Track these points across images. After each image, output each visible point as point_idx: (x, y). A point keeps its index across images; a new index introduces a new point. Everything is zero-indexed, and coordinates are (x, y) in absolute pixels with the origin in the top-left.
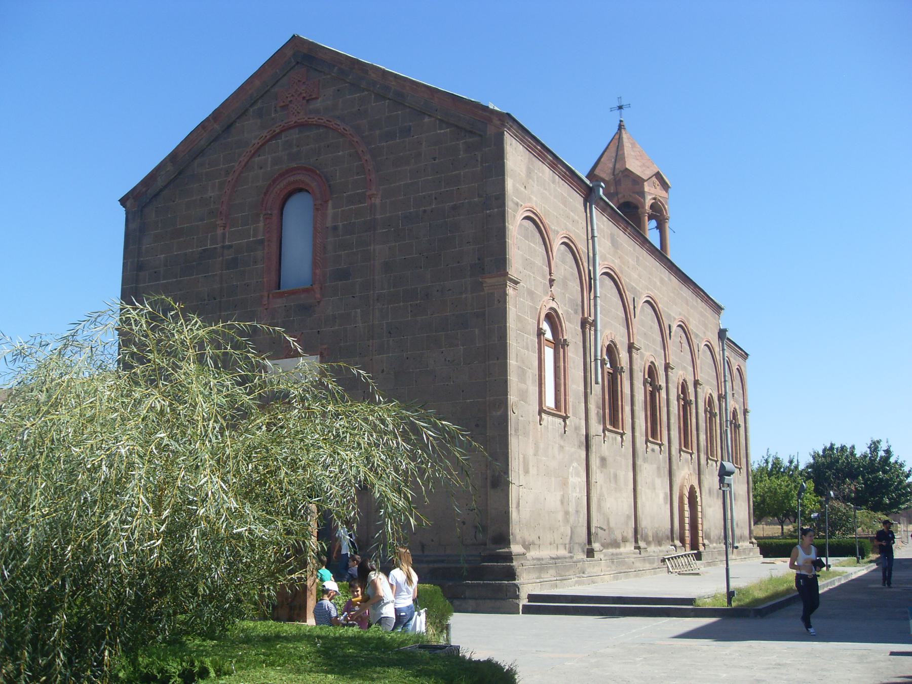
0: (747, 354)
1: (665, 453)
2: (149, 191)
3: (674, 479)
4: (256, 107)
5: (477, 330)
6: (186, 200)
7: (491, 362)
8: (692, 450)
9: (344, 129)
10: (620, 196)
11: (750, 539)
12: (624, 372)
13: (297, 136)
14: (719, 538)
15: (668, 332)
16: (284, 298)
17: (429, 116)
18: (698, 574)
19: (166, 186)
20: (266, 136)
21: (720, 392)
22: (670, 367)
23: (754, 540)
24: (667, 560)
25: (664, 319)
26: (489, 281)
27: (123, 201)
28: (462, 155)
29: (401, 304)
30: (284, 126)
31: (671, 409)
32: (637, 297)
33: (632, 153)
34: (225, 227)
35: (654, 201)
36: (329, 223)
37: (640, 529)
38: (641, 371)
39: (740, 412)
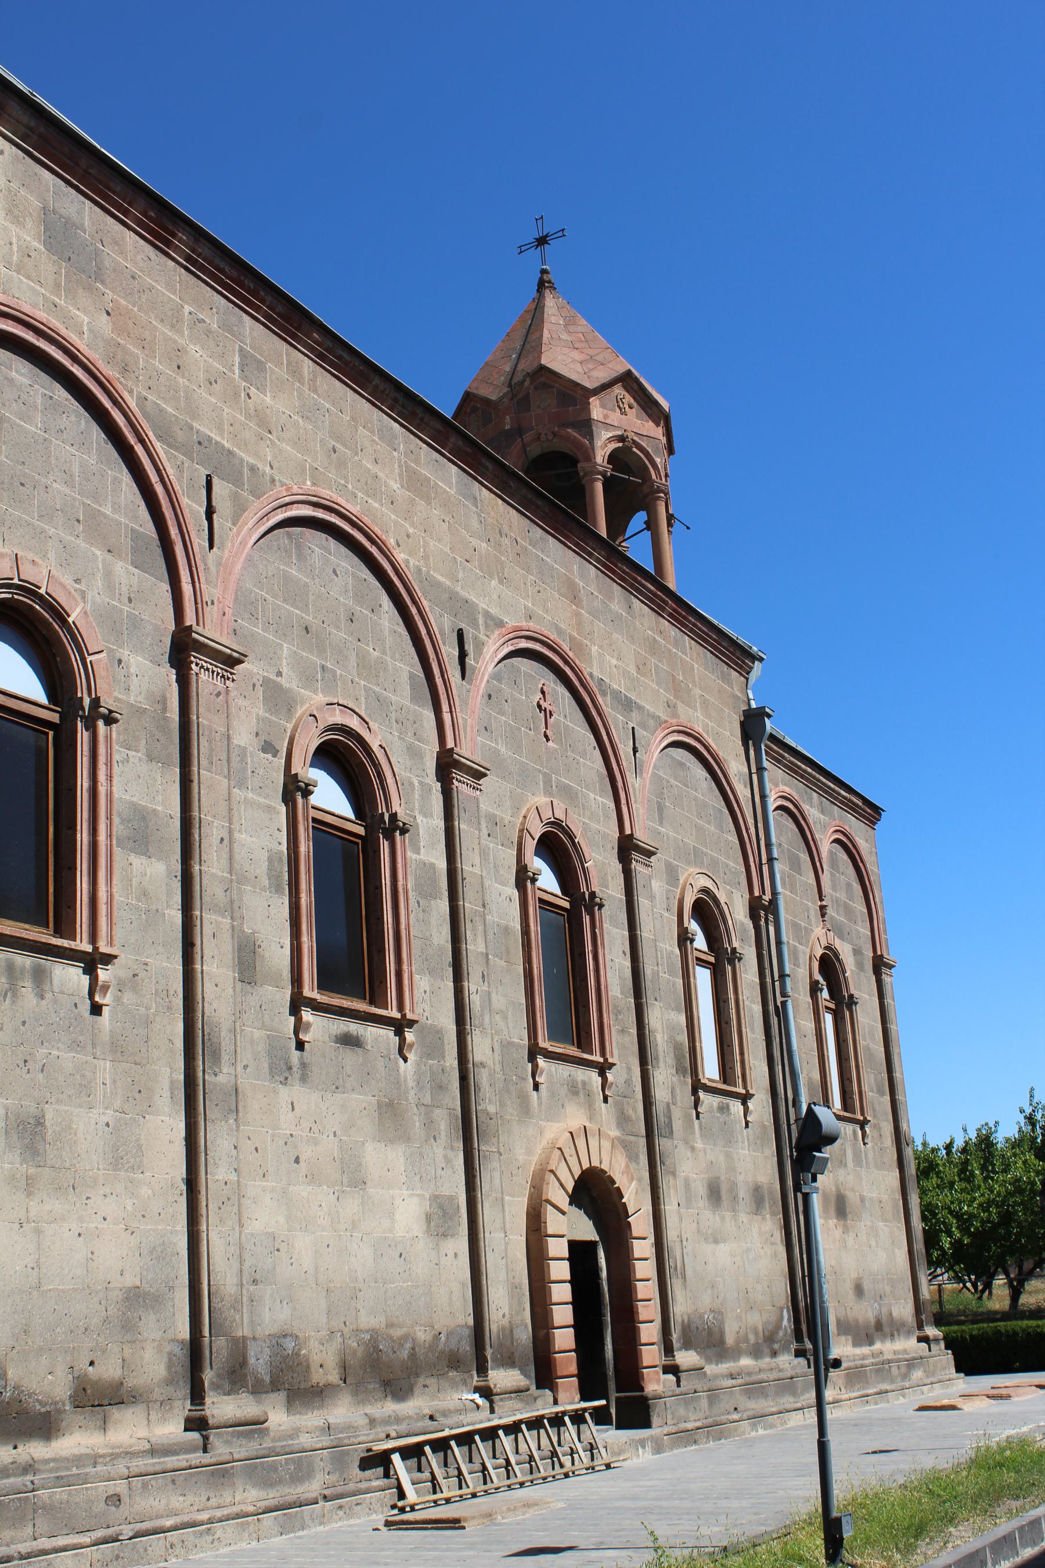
0: (877, 810)
1: (433, 1049)
3: (484, 1148)
8: (603, 1053)
10: (528, 437)
11: (920, 1326)
12: (110, 720)
14: (770, 1338)
15: (450, 651)
18: (454, 1524)
21: (757, 894)
22: (457, 765)
23: (931, 1331)
24: (396, 1458)
25: (425, 603)
31: (469, 905)
32: (237, 481)
33: (564, 336)
35: (621, 445)
37: (221, 1343)
38: (268, 748)
39: (860, 966)
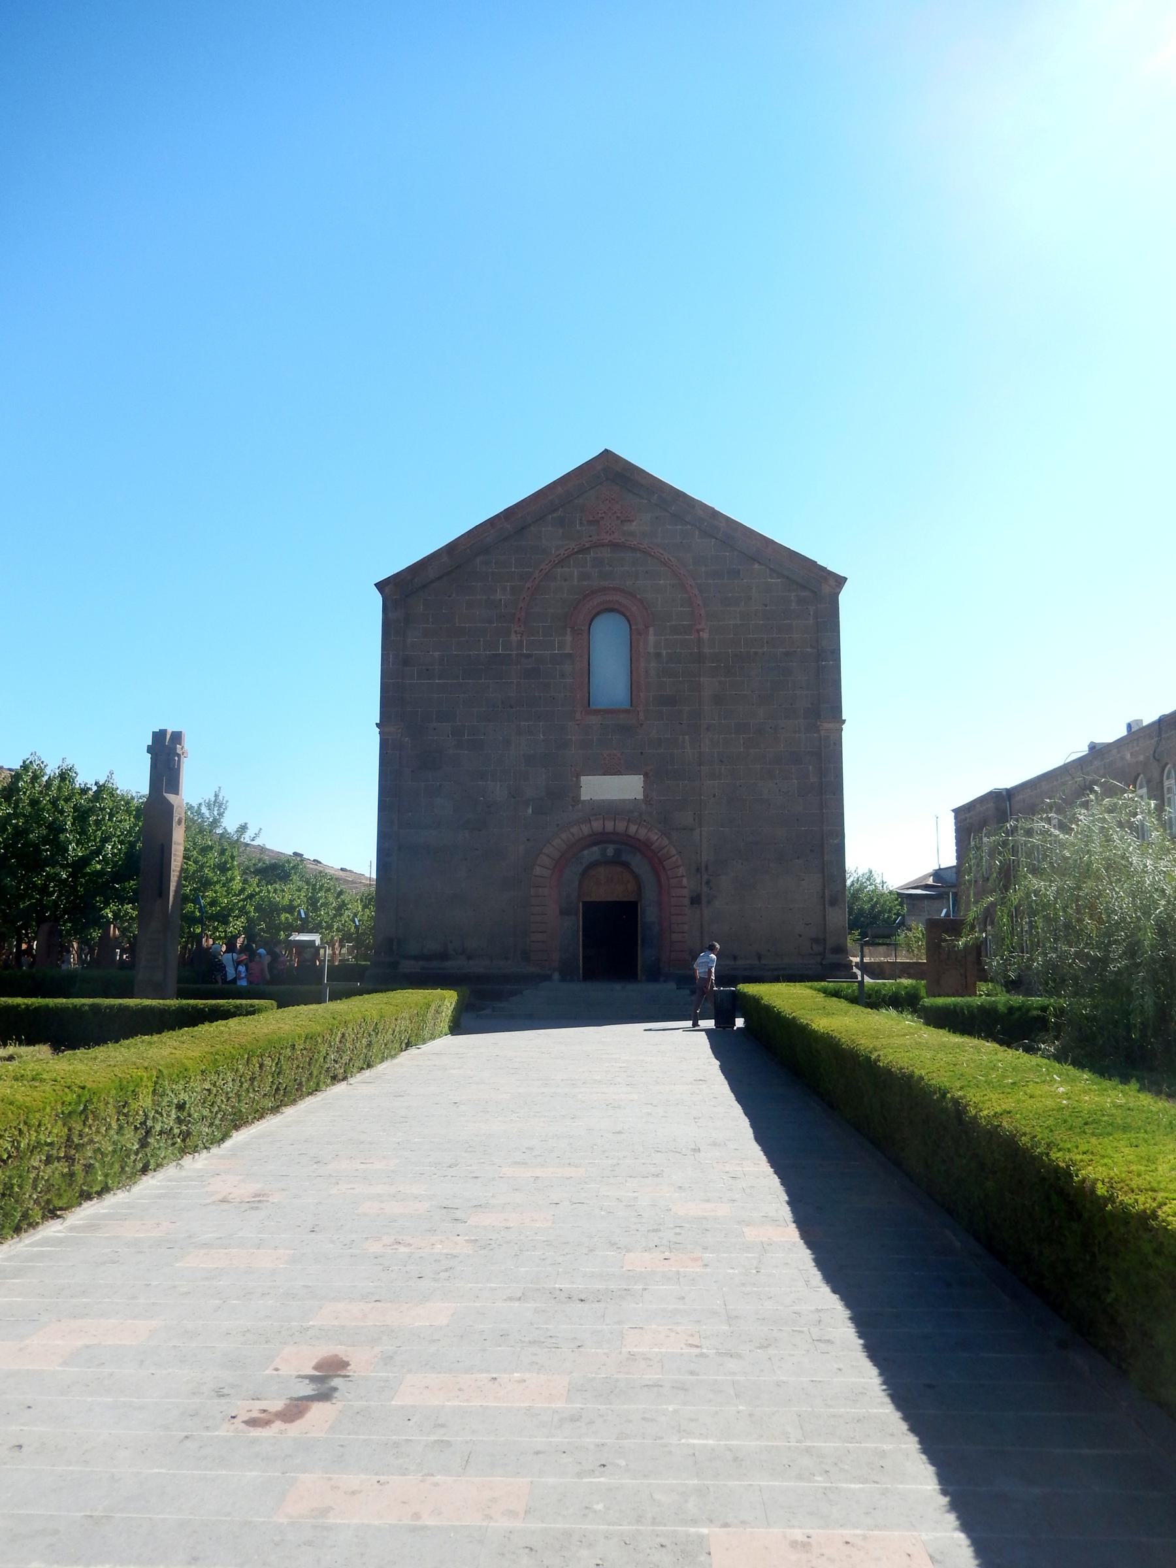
2: (416, 580)
4: (555, 515)
5: (811, 767)
6: (467, 598)
7: (828, 797)
9: (668, 559)
13: (609, 555)
16: (599, 716)
17: (759, 562)
19: (440, 578)
20: (573, 549)
26: (826, 725)
27: (380, 586)
28: (794, 606)
29: (733, 736)
30: (595, 543)
34: (522, 634)
36: (651, 650)
